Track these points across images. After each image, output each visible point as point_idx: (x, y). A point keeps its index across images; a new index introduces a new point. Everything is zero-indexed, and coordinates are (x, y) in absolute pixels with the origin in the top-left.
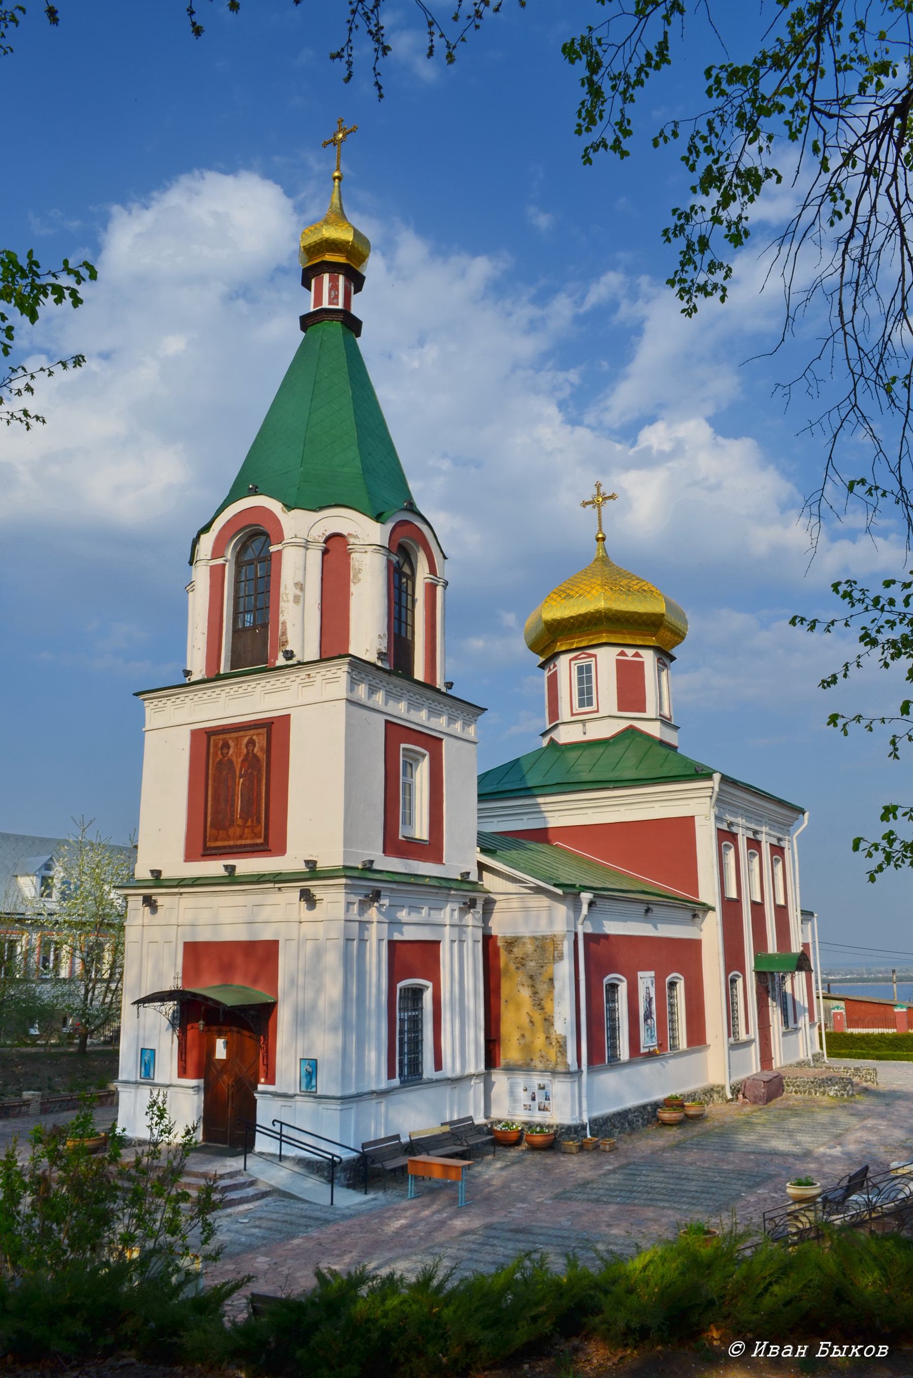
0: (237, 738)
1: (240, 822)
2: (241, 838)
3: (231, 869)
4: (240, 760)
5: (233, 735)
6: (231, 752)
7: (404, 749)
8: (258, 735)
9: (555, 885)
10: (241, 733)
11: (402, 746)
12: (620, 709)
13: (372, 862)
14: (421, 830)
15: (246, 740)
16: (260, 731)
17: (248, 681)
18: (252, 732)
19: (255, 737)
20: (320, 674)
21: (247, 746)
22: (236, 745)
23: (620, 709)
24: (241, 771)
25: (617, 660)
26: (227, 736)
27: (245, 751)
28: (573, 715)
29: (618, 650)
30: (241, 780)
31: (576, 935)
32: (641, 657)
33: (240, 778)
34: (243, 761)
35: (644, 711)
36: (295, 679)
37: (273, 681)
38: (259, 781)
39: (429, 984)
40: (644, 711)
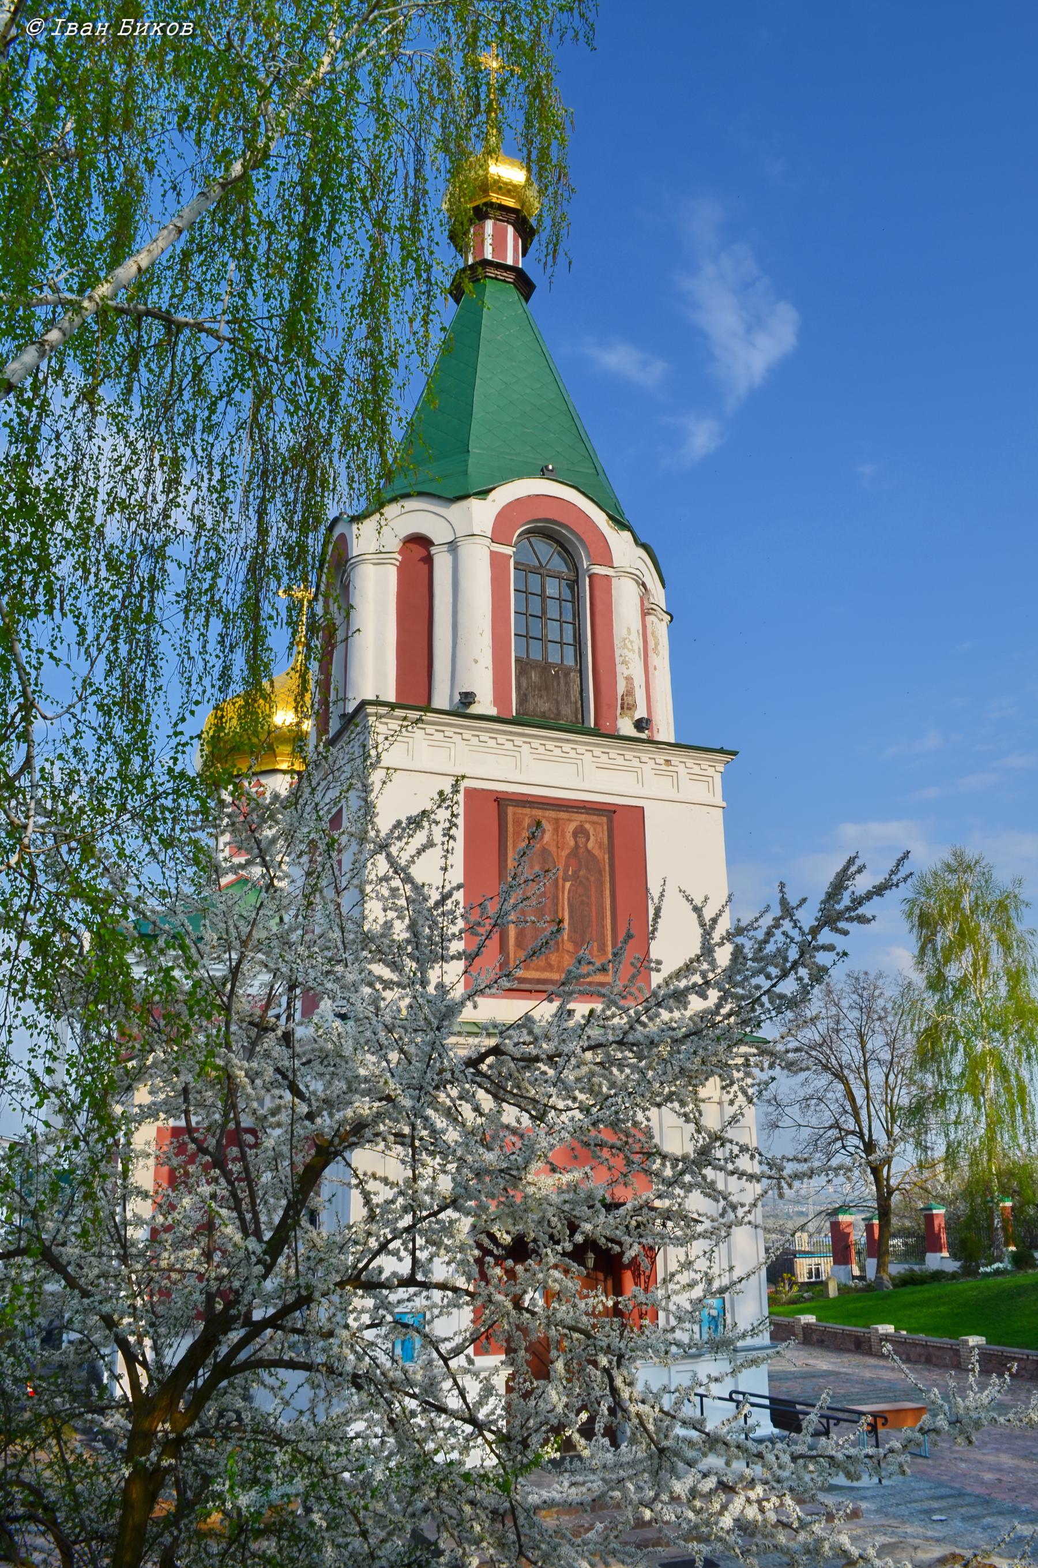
0: (557, 820)
1: (569, 946)
4: (564, 853)
5: (547, 813)
6: (547, 837)
8: (593, 823)
10: (563, 815)
15: (572, 827)
16: (594, 818)
17: (511, 733)
18: (583, 817)
19: (587, 826)
20: (685, 764)
21: (575, 834)
22: (556, 830)
24: (566, 871)
26: (538, 813)
27: (572, 843)
30: (568, 885)
33: (565, 880)
34: (568, 856)
36: (648, 761)
37: (613, 754)
38: (602, 892)
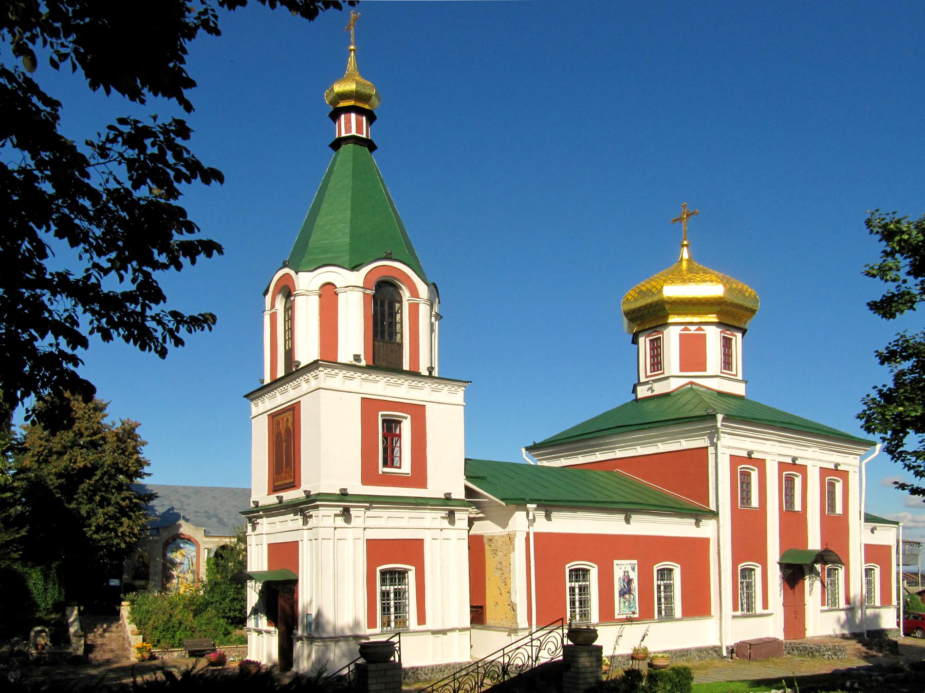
2: (286, 479)
3: (280, 499)
7: (382, 415)
9: (502, 500)
11: (380, 413)
12: (681, 370)
13: (345, 490)
14: (406, 468)
23: (681, 370)
25: (681, 335)
28: (647, 377)
29: (683, 327)
31: (528, 534)
32: (702, 330)
35: (705, 370)
39: (413, 568)
40: (705, 370)
